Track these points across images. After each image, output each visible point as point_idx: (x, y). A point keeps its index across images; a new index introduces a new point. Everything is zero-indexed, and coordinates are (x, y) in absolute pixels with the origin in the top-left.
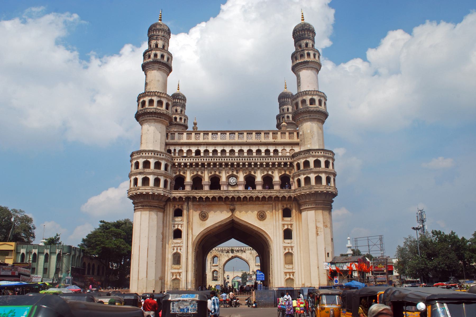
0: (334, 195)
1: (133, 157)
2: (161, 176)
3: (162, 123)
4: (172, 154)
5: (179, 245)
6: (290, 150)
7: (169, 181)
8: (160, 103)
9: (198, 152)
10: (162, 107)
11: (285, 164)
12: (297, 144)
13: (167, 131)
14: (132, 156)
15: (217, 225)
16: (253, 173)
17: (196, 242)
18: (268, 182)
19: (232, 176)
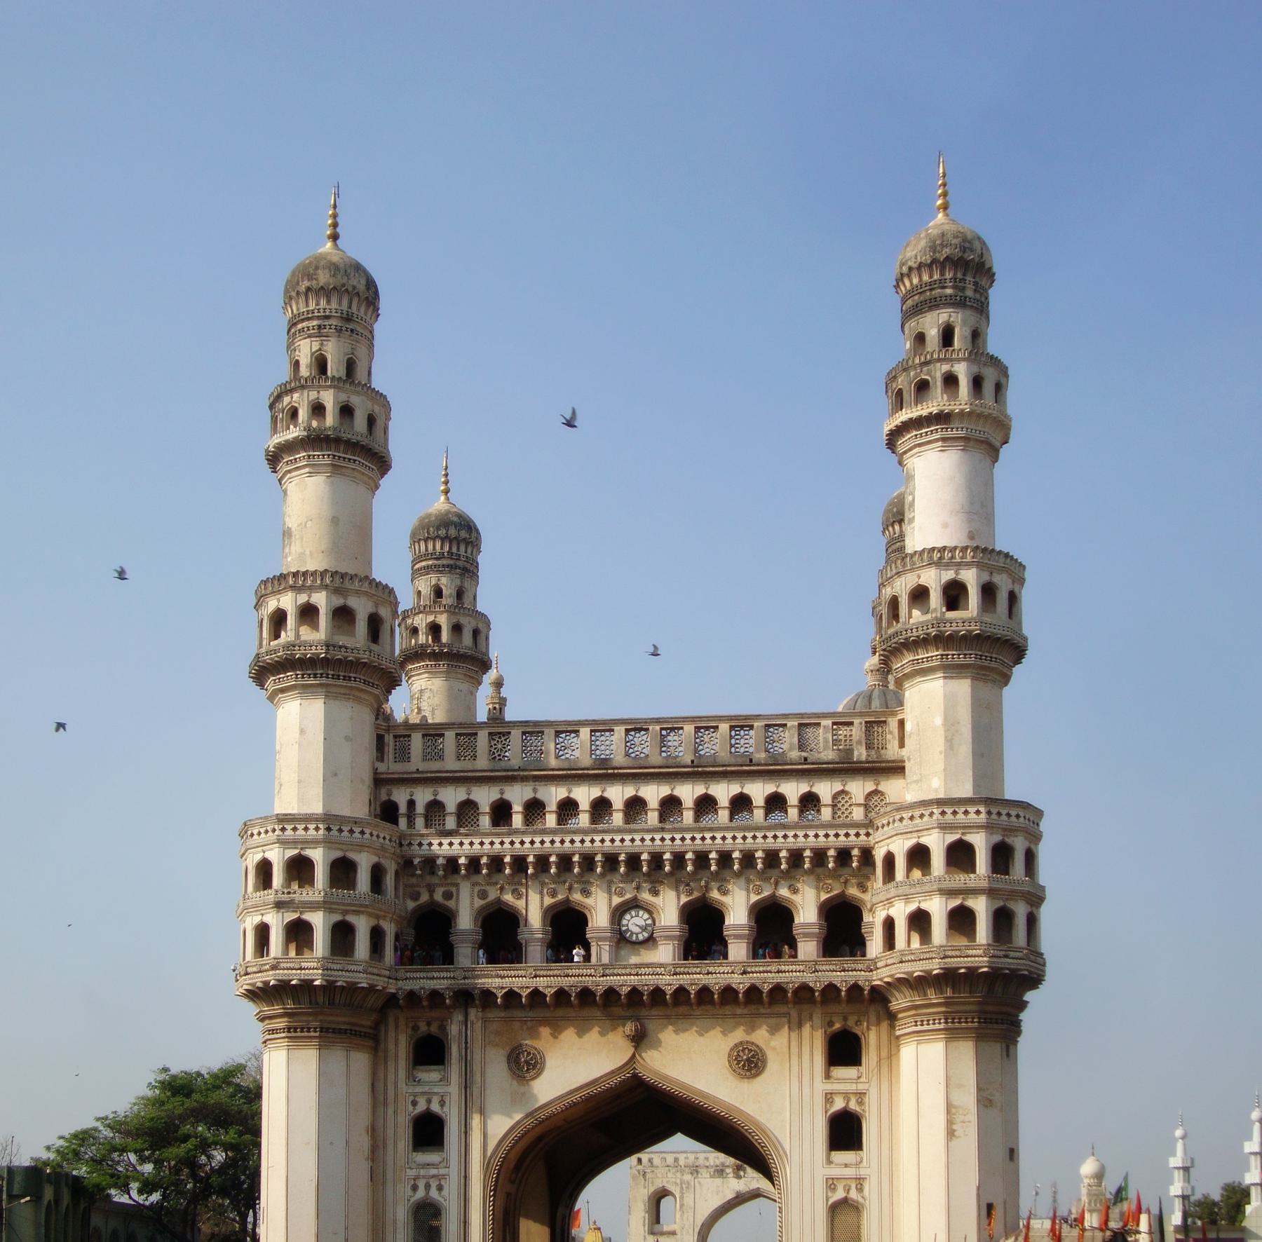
1: (250, 842)
2: (357, 913)
3: (358, 700)
5: (433, 1172)
6: (870, 795)
7: (390, 929)
10: (353, 635)
11: (844, 855)
12: (897, 769)
13: (377, 727)
15: (576, 1098)
17: (497, 1161)
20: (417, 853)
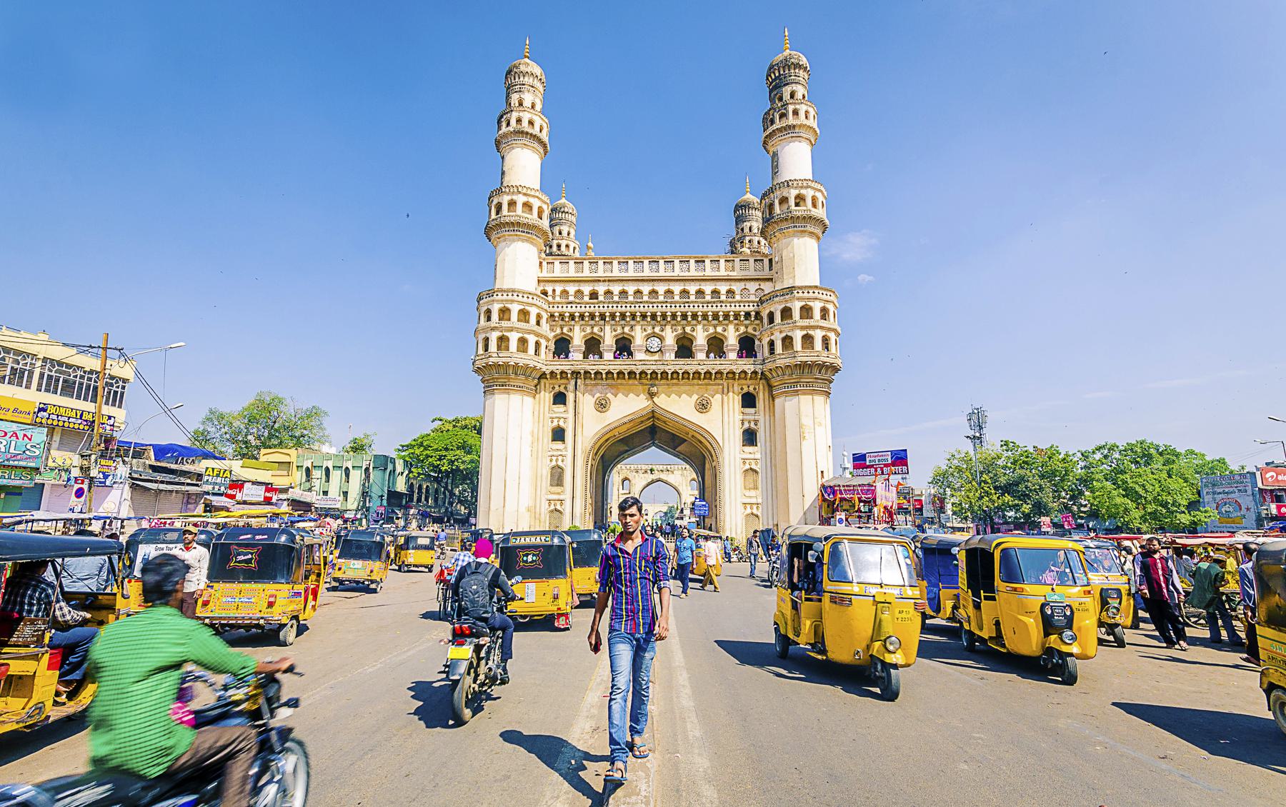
0: (836, 369)
4: (550, 299)
8: (527, 206)
9: (594, 295)
11: (748, 315)
14: (480, 299)
16: (688, 329)
18: (716, 345)
19: (654, 335)
20: (556, 311)
